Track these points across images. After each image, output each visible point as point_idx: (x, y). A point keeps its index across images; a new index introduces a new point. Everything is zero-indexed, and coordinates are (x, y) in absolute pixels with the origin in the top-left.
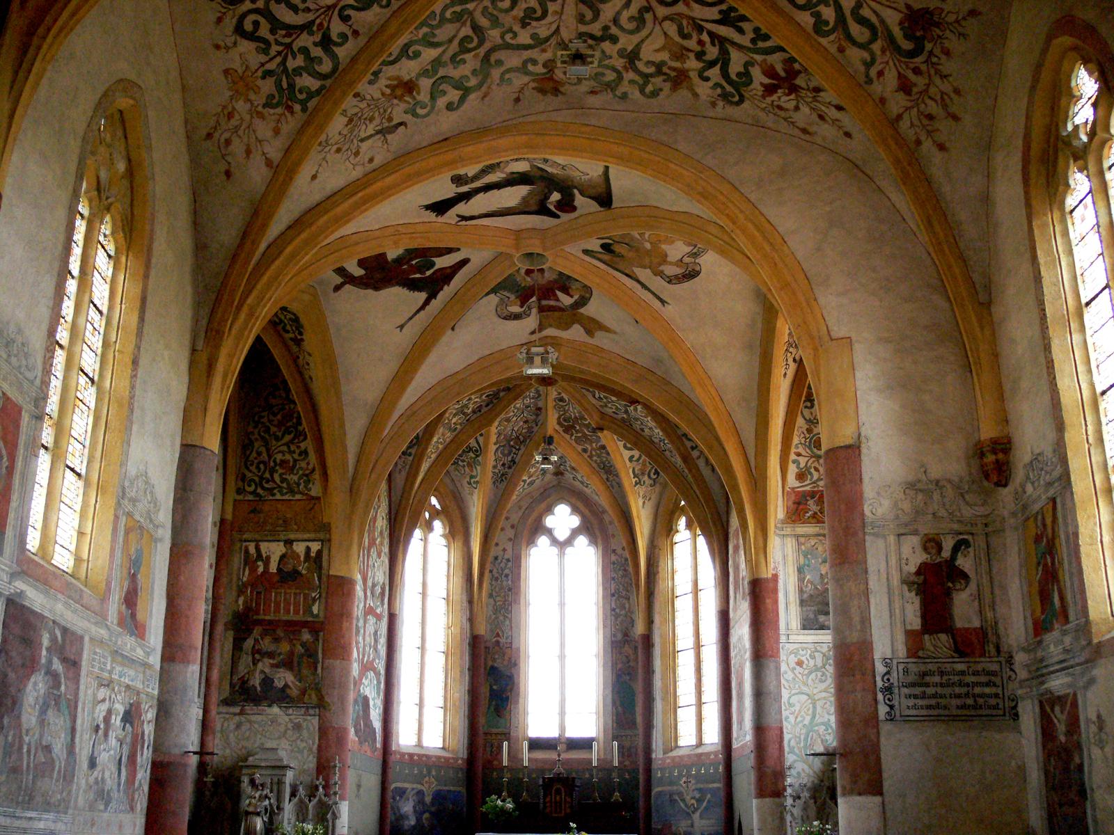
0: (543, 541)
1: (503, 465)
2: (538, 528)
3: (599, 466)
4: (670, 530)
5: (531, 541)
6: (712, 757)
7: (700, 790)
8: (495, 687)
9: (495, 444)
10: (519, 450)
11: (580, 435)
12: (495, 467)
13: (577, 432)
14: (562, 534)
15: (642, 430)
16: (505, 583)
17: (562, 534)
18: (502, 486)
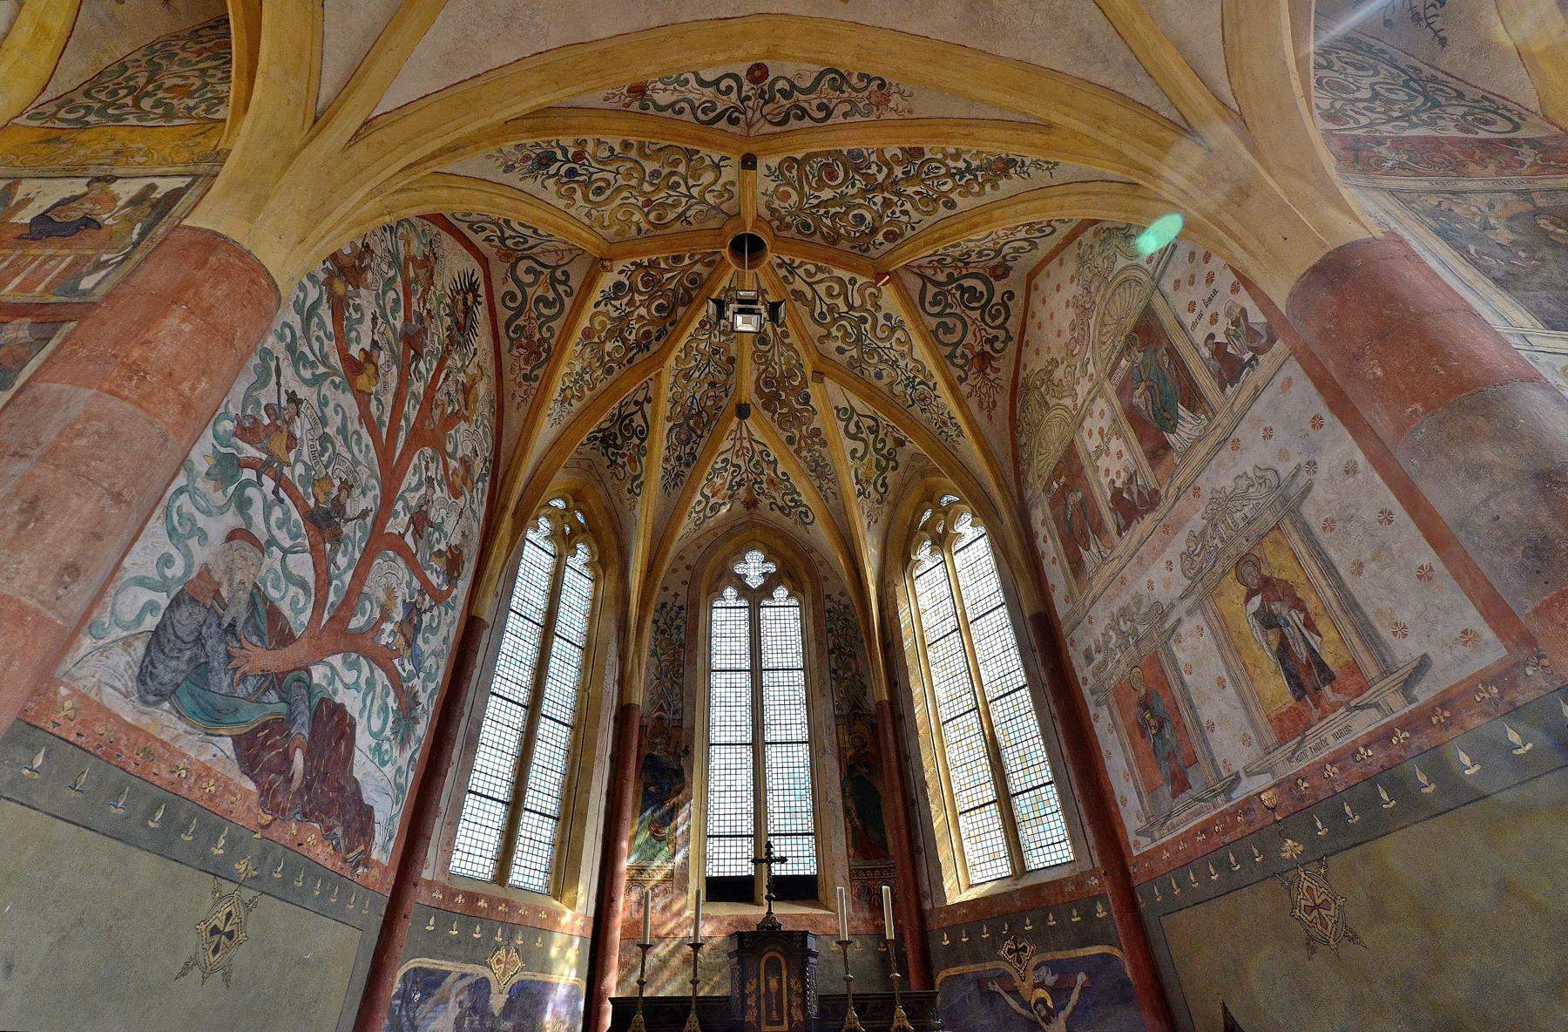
0: (730, 592)
1: (679, 458)
2: (725, 576)
3: (809, 466)
4: (906, 561)
5: (715, 592)
6: (1070, 888)
7: (1054, 966)
8: (652, 789)
9: (669, 419)
10: (701, 437)
11: (785, 410)
12: (666, 460)
13: (783, 404)
14: (755, 581)
15: (879, 376)
16: (674, 637)
17: (755, 581)
18: (677, 492)
